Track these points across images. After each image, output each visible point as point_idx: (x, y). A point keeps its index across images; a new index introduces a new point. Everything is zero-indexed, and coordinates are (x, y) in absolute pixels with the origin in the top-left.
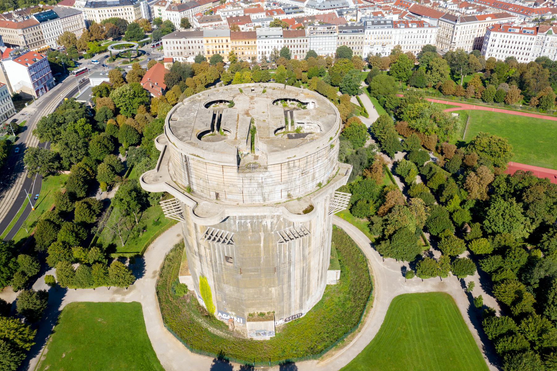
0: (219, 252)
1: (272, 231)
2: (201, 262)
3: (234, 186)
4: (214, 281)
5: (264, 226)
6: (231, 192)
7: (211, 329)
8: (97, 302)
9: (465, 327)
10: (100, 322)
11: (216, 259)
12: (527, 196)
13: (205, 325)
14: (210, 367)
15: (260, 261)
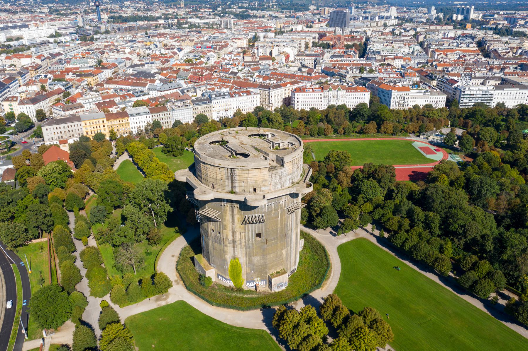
0: (252, 232)
1: (285, 207)
2: (234, 247)
3: (266, 180)
4: (246, 257)
5: (281, 205)
6: (264, 186)
7: (245, 296)
8: (148, 310)
9: (382, 249)
10: (163, 320)
11: (249, 238)
12: (378, 175)
13: (240, 295)
14: (261, 314)
15: (277, 231)
